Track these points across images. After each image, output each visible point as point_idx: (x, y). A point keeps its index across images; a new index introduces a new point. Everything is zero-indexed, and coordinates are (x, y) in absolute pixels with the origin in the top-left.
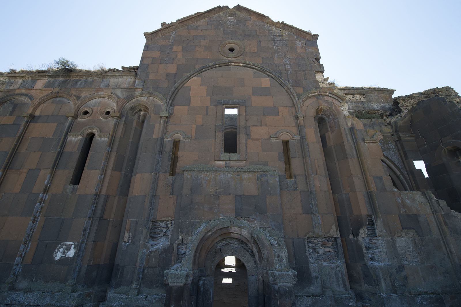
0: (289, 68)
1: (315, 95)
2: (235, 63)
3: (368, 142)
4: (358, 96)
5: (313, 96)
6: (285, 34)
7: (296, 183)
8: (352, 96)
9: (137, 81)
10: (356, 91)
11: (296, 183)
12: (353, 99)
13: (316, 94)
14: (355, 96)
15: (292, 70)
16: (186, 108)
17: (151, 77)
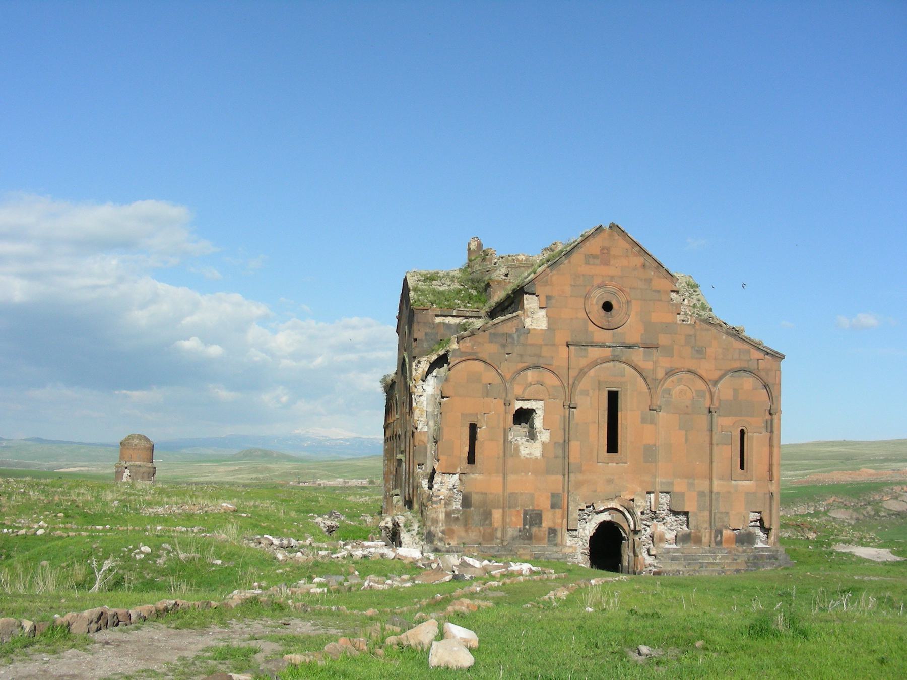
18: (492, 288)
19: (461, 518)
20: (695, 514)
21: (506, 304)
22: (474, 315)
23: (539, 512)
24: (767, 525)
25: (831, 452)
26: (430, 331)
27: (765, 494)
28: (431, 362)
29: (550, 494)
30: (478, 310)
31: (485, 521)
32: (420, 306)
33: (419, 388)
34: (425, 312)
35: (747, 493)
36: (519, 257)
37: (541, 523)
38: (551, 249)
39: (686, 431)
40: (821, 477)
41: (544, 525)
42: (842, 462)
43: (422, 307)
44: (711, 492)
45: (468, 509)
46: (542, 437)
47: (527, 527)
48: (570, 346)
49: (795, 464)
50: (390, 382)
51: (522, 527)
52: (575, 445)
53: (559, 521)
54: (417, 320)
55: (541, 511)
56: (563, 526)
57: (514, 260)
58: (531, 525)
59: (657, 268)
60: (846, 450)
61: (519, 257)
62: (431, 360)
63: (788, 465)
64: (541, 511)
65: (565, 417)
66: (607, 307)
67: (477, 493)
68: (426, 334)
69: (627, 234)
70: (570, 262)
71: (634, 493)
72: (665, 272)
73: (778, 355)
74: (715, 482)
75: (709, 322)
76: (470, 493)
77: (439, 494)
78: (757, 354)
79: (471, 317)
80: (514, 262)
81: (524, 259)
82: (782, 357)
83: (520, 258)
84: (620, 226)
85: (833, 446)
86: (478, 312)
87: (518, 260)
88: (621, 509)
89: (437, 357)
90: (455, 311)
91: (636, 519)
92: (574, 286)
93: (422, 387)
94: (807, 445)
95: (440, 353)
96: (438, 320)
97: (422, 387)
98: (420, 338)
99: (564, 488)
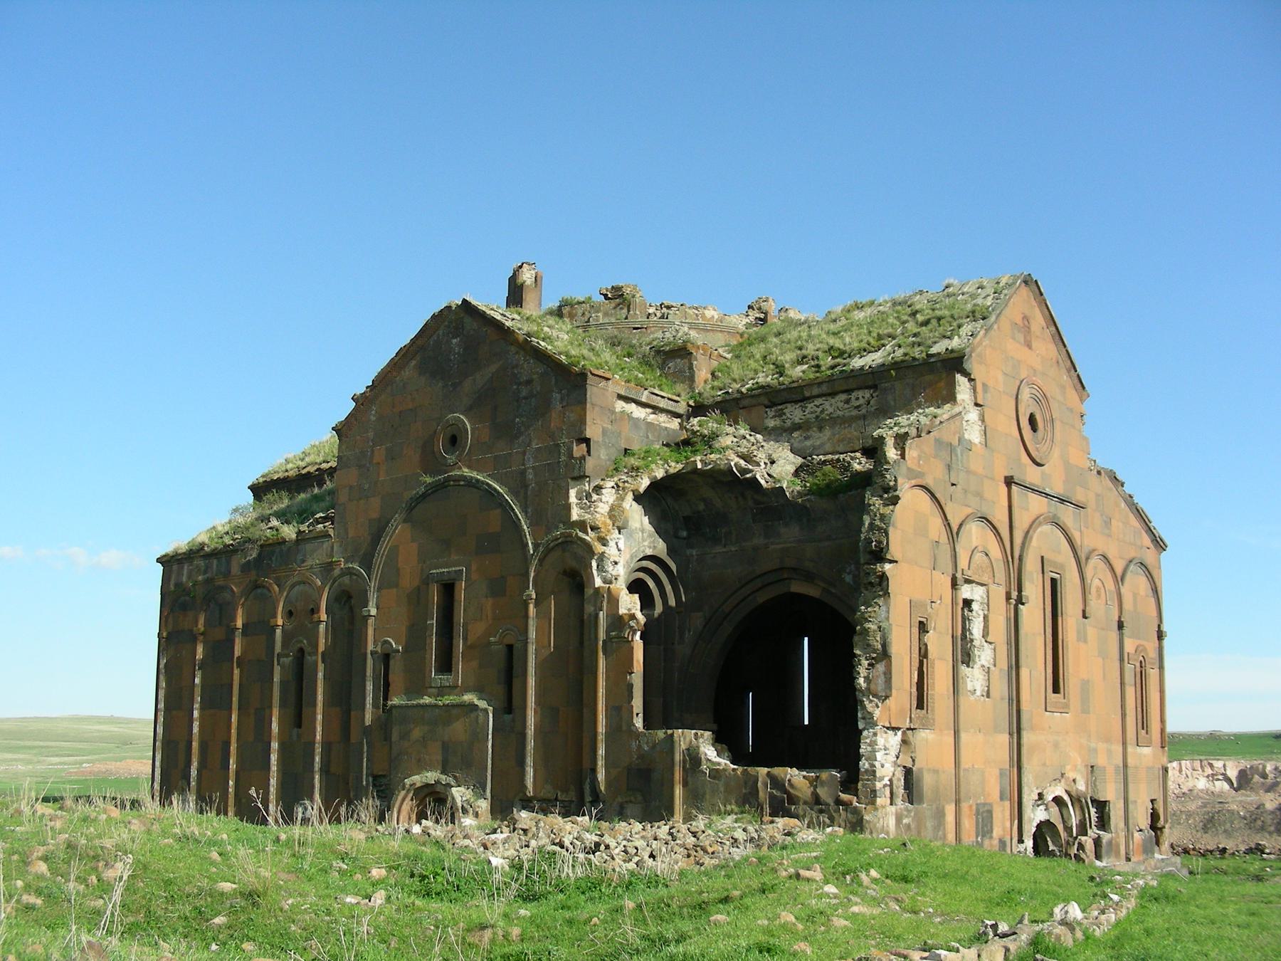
0: (531, 477)
1: (560, 543)
2: (453, 481)
3: (616, 640)
4: (860, 393)
5: (557, 545)
6: (537, 373)
7: (513, 720)
8: (843, 397)
9: (335, 545)
10: (851, 380)
11: (513, 720)
12: (846, 406)
13: (560, 541)
14: (854, 394)
15: (535, 483)
16: (395, 590)
17: (351, 533)
18: (697, 360)
19: (913, 826)
20: (1114, 804)
21: (816, 391)
22: (670, 408)
23: (989, 808)
24: (1161, 823)
25: (99, 731)
26: (610, 427)
27: (1159, 768)
28: (642, 490)
29: (997, 772)
30: (677, 398)
31: (938, 831)
32: (598, 368)
33: (612, 544)
34: (603, 383)
35: (1148, 768)
36: (706, 312)
37: (992, 832)
38: (760, 309)
39: (1103, 659)
40: (112, 766)
41: (995, 834)
42: (118, 747)
43: (600, 372)
44: (1125, 766)
45: (920, 806)
46: (982, 658)
47: (979, 839)
48: (1014, 487)
49: (52, 747)
50: (294, 536)
51: (975, 840)
52: (1024, 673)
53: (1008, 824)
54: (591, 398)
55: (991, 805)
56: (1013, 835)
57: (697, 315)
58: (983, 836)
59: (1069, 371)
60: (121, 730)
61: (706, 312)
62: (639, 487)
63: (42, 747)
64: (991, 805)
65: (1008, 619)
66: (1032, 421)
67: (929, 770)
68: (604, 432)
69: (1045, 300)
70: (999, 328)
71: (1075, 768)
72: (1076, 381)
73: (1162, 544)
74: (1130, 749)
75: (1115, 477)
76: (920, 770)
77: (884, 774)
78: (1147, 541)
79: (662, 411)
80: (698, 320)
81: (716, 317)
82: (1165, 547)
83: (709, 313)
84: (1039, 283)
85: (100, 723)
86: (677, 402)
87: (703, 316)
88: (1066, 798)
89: (648, 483)
90: (646, 393)
91: (1087, 815)
92: (1005, 374)
93: (617, 543)
94: (62, 719)
95: (657, 474)
96: (620, 405)
97: (617, 543)
98: (596, 439)
99: (1011, 758)
